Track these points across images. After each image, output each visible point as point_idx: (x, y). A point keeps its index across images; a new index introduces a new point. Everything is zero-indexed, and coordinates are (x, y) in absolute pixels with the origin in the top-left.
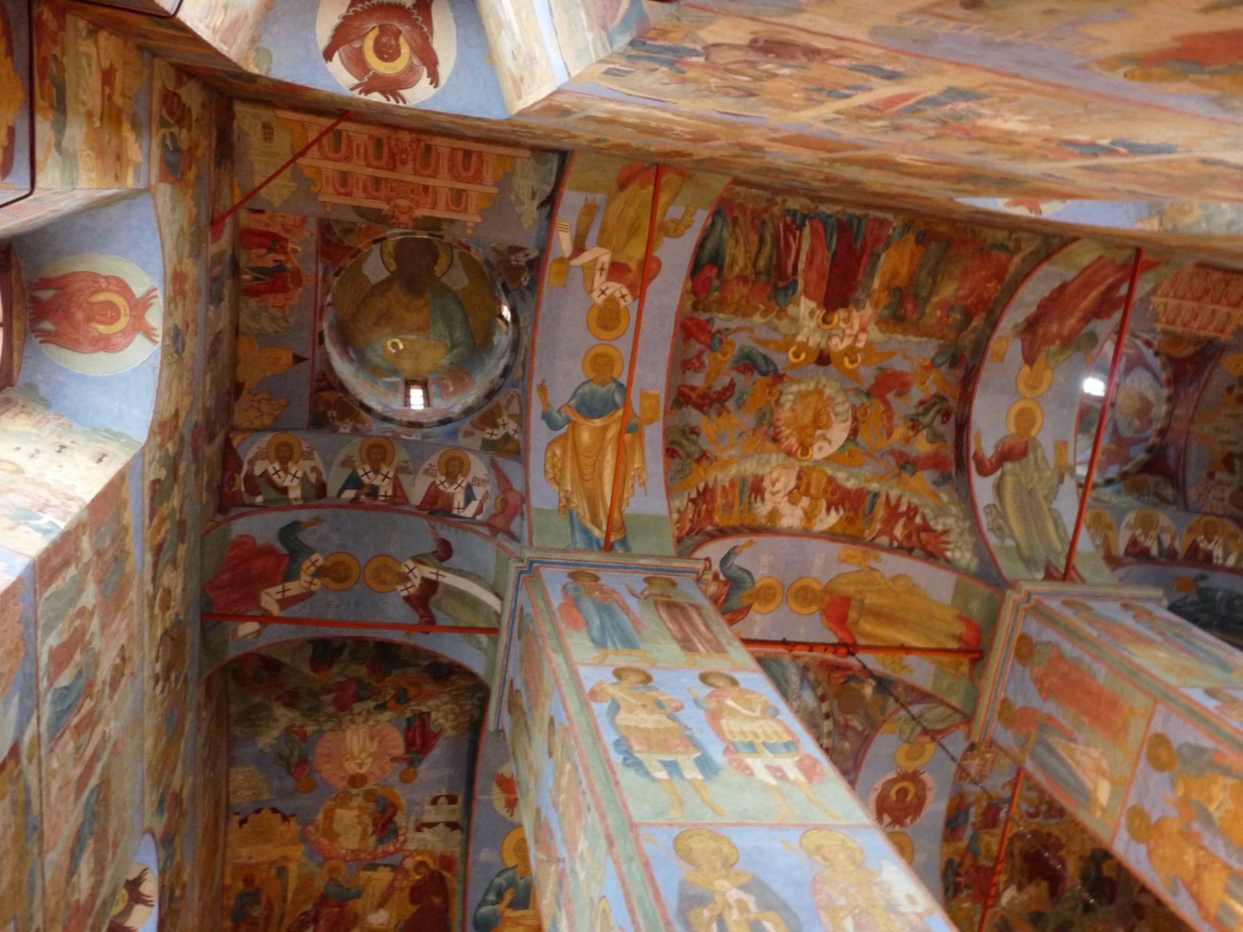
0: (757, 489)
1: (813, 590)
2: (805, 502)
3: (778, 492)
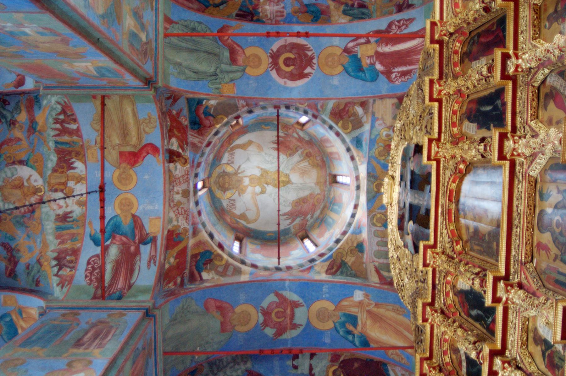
0: (64, 218)
2: (71, 184)
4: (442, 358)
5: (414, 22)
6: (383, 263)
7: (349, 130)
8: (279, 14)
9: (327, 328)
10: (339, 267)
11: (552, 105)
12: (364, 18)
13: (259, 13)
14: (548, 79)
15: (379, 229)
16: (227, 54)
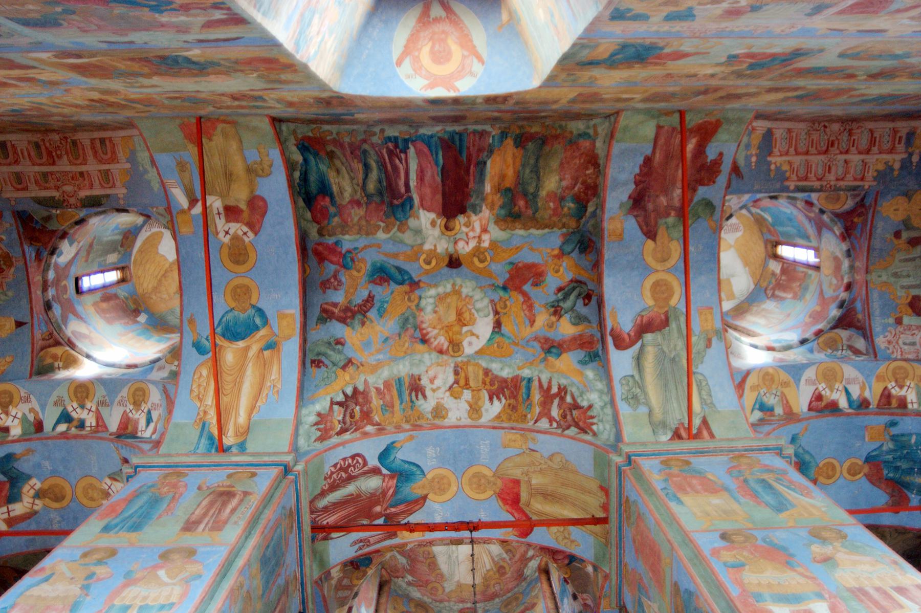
0: (416, 388)
1: (484, 476)
2: (467, 395)
3: (439, 388)
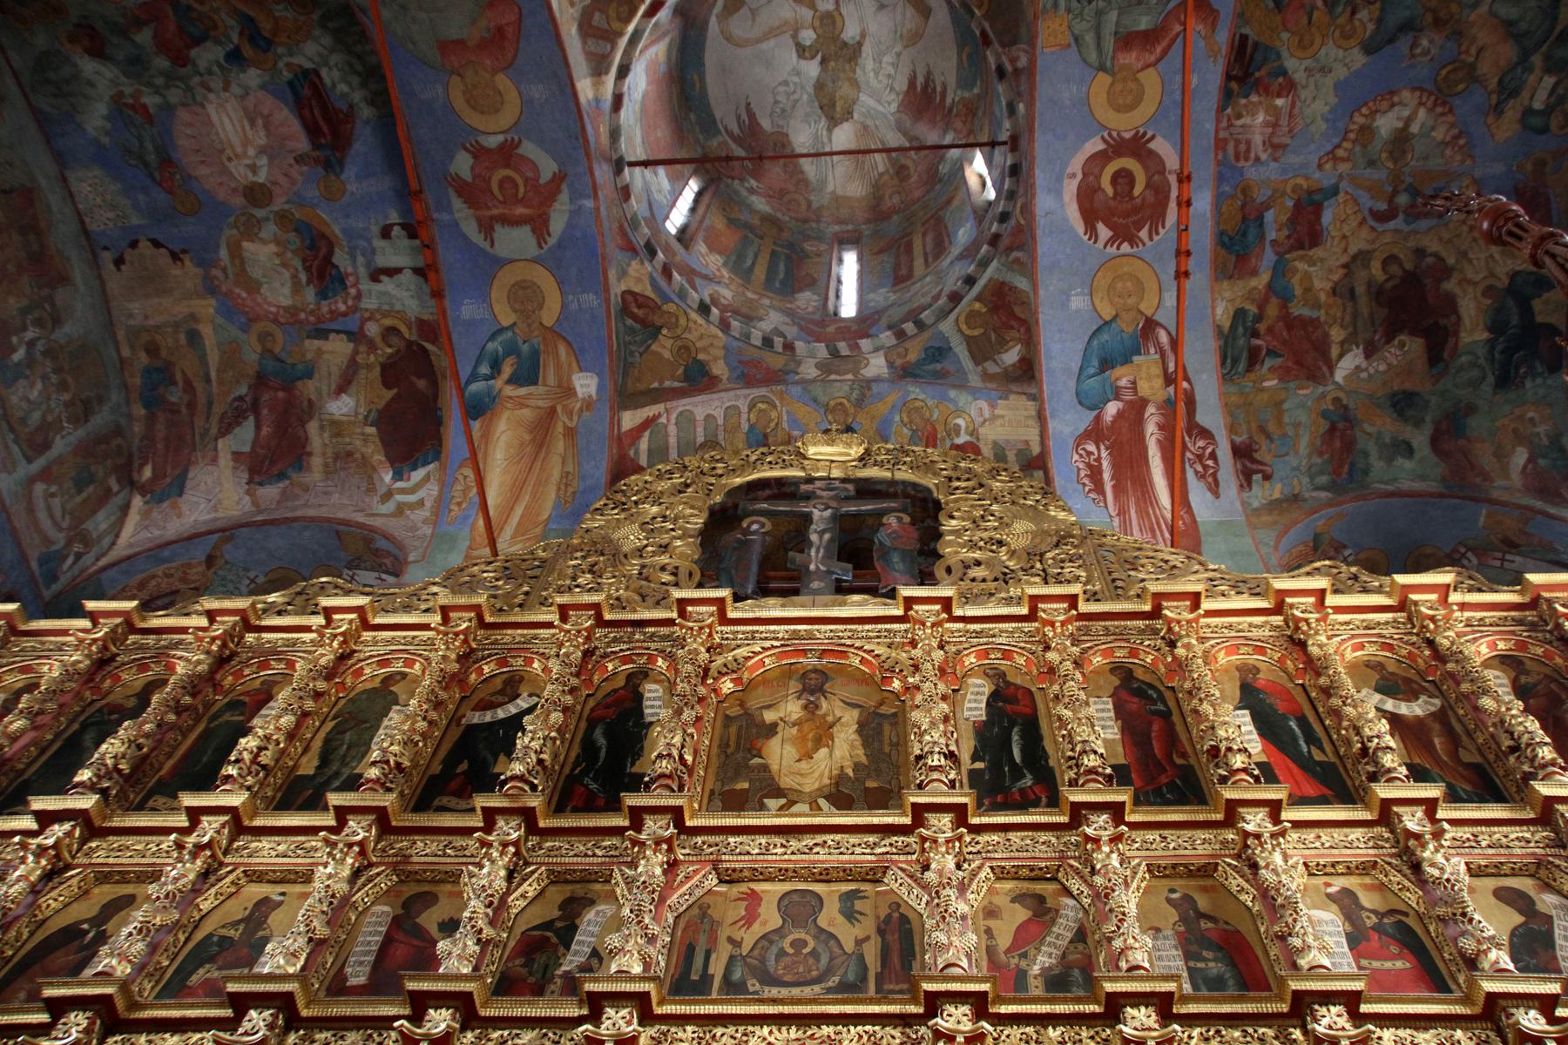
4: (490, 656)
5: (1209, 495)
6: (667, 435)
7: (964, 327)
8: (1242, 147)
9: (497, 309)
10: (643, 322)
11: (1022, 914)
12: (1223, 364)
13: (1246, 97)
14: (1071, 902)
15: (744, 416)
16: (1144, 23)
